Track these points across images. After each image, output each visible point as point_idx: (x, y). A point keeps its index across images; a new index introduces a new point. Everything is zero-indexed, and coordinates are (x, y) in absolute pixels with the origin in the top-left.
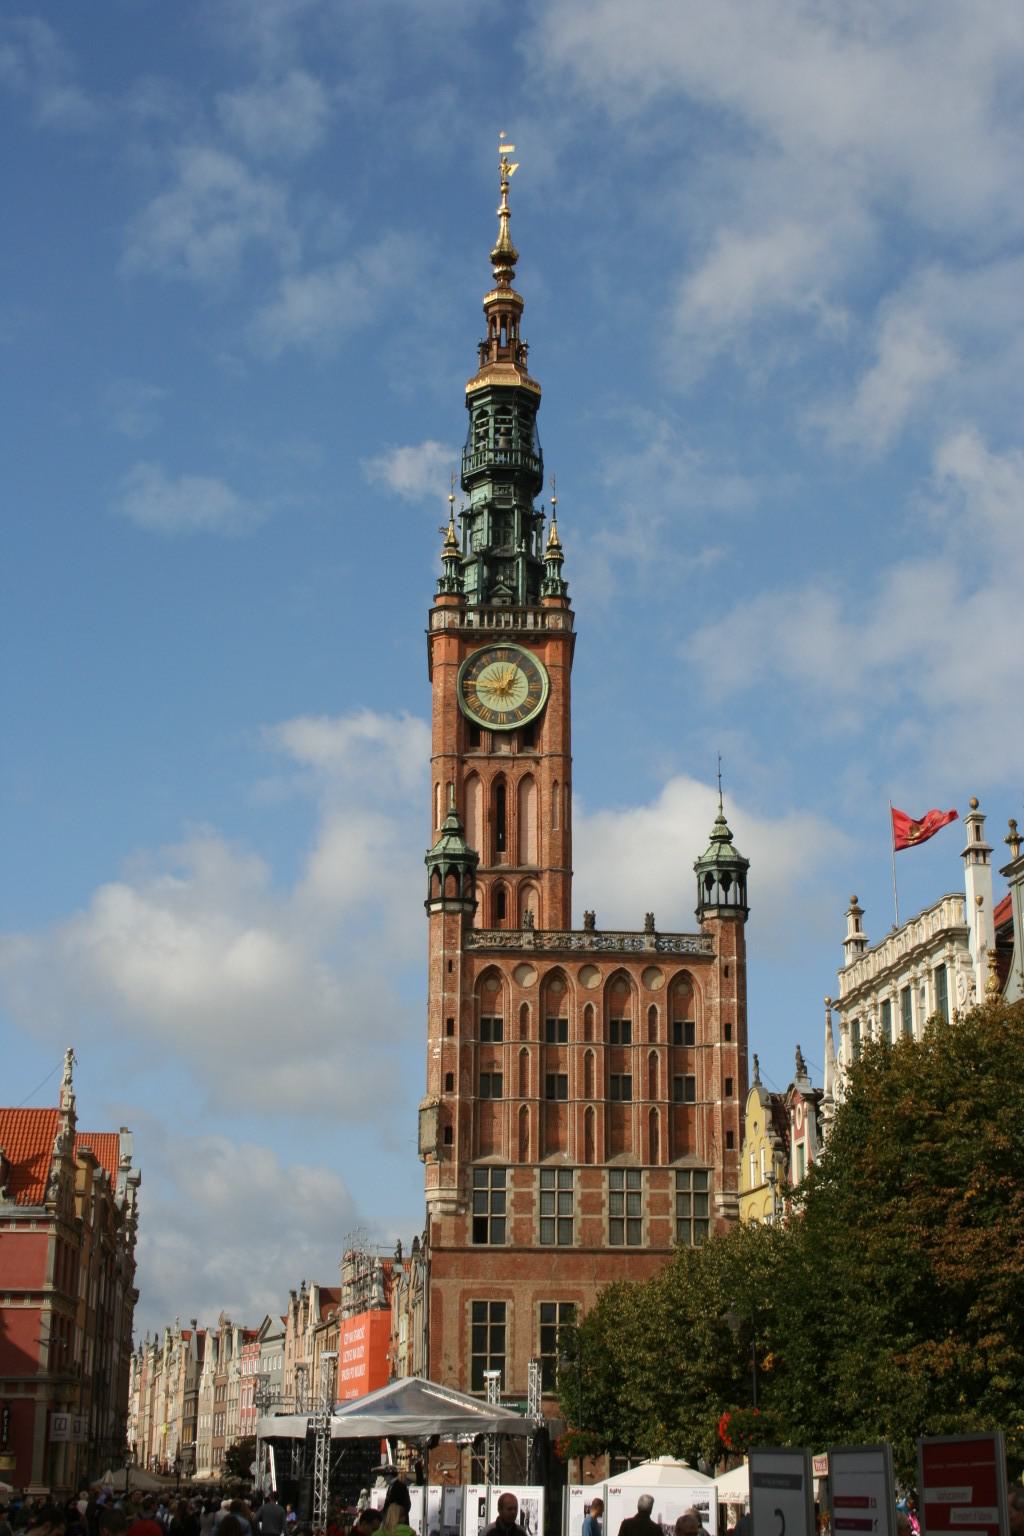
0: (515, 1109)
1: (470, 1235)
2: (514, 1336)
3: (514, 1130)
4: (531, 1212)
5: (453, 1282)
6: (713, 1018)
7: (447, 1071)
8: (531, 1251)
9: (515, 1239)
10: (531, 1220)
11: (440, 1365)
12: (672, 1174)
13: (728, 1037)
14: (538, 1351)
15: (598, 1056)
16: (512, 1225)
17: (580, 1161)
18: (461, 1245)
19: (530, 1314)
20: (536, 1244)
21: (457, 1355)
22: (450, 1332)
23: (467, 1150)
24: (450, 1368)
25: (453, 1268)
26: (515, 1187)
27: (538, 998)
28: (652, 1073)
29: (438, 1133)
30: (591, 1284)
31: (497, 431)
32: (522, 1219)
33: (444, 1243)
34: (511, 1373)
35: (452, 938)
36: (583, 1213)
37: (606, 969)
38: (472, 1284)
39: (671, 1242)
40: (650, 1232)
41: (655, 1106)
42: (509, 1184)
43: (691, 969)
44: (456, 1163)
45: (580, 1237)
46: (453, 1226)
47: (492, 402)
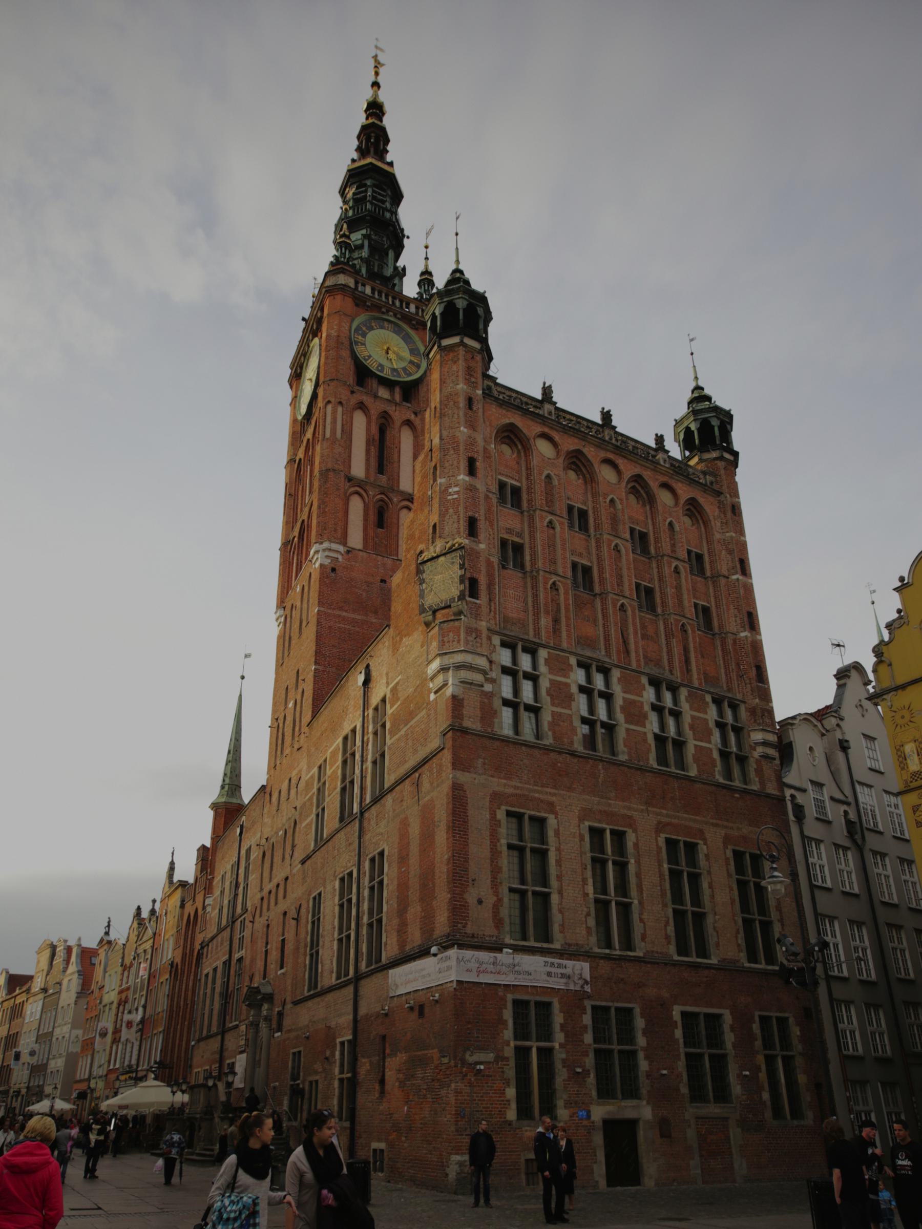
0: (546, 583)
2: (560, 866)
3: (545, 604)
7: (470, 514)
8: (573, 754)
9: (555, 738)
10: (571, 716)
11: (466, 896)
12: (708, 698)
14: (590, 889)
15: (627, 555)
16: (550, 719)
17: (619, 661)
18: (489, 730)
19: (577, 840)
20: (579, 747)
21: (489, 881)
22: (479, 850)
24: (480, 902)
28: (678, 588)
29: (462, 579)
30: (642, 811)
31: (374, 198)
32: (560, 714)
33: (467, 723)
34: (560, 916)
36: (627, 722)
37: (629, 469)
38: (505, 785)
39: (717, 777)
40: (696, 760)
41: (685, 621)
42: (543, 668)
43: (701, 500)
44: (484, 624)
45: (625, 750)
47: (371, 178)
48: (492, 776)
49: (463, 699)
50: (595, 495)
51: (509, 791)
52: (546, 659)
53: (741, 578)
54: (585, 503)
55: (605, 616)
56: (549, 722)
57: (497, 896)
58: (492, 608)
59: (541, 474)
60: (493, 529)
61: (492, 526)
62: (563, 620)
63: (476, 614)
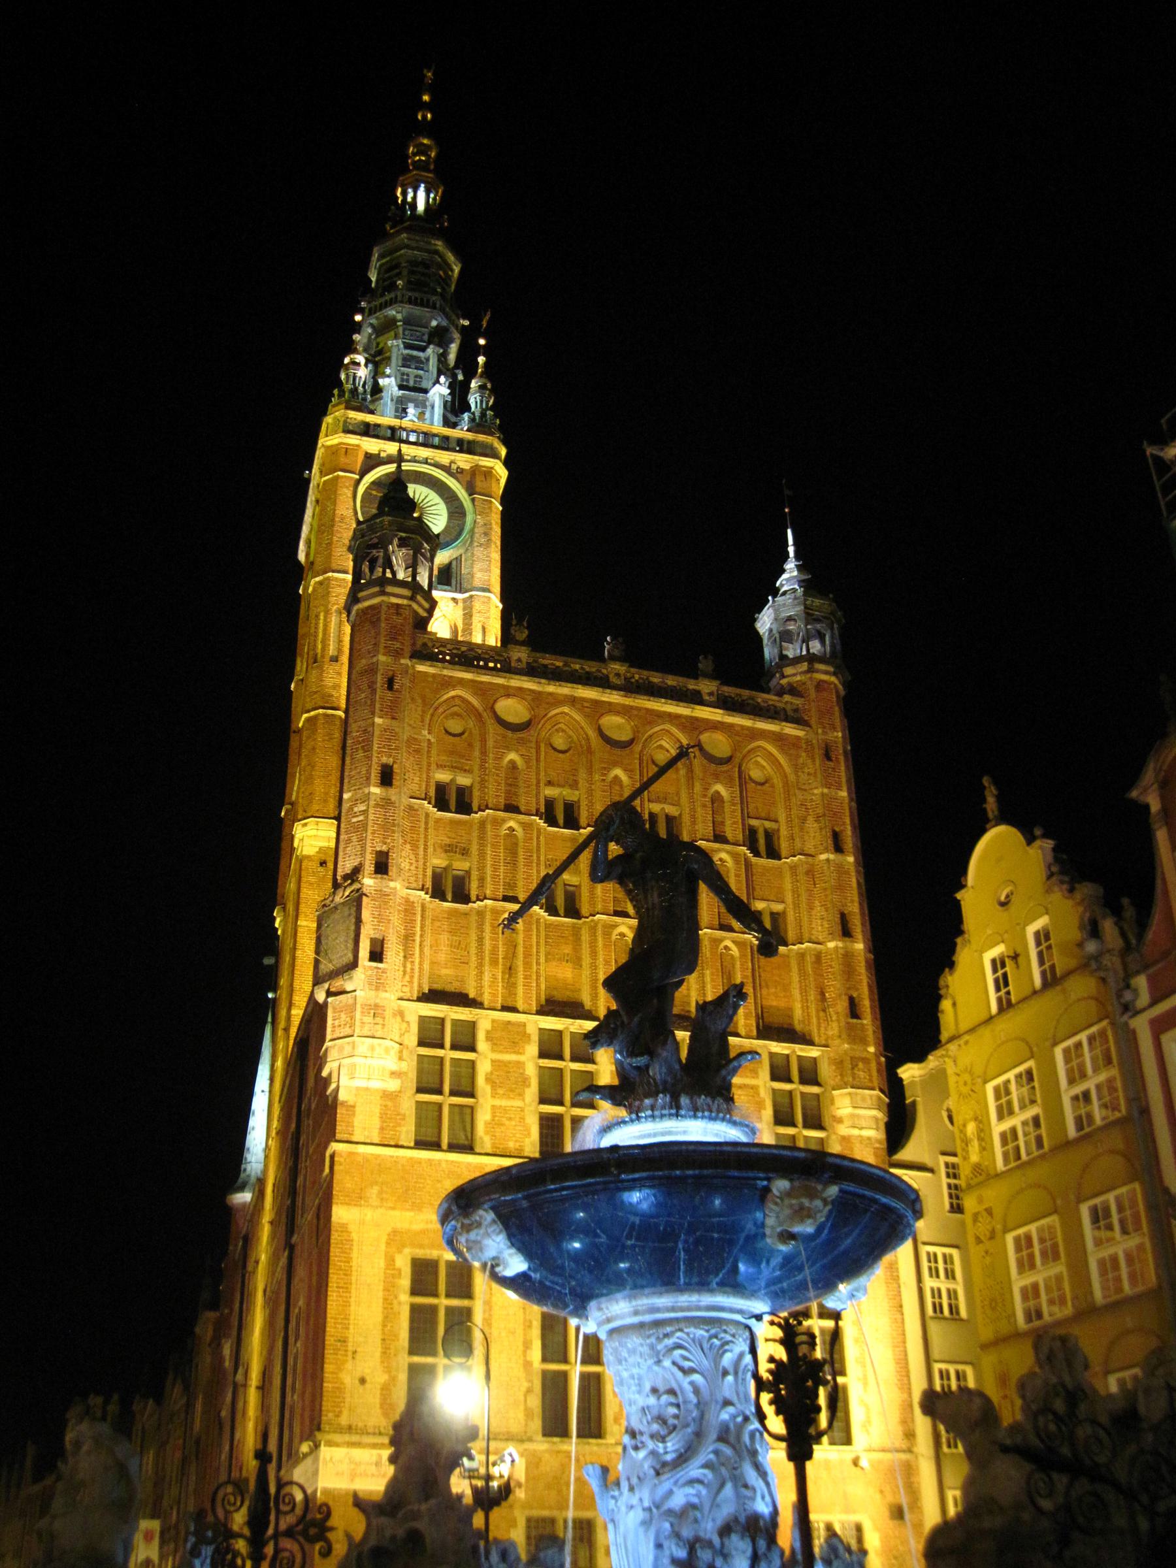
1: (407, 1132)
3: (494, 950)
4: (521, 1095)
5: (369, 1214)
6: (810, 819)
13: (838, 848)
14: (536, 1354)
16: (488, 1117)
21: (378, 1354)
23: (407, 978)
25: (375, 1190)
26: (493, 1050)
27: (533, 751)
32: (505, 1110)
35: (394, 639)
46: (377, 1110)
48: (393, 1208)
49: (354, 1107)
50: (590, 771)
51: (416, 1227)
52: (488, 1032)
53: (832, 856)
54: (574, 785)
55: (594, 954)
56: (487, 1124)
57: (389, 1372)
58: (408, 970)
59: (499, 758)
60: (416, 855)
61: (415, 848)
62: (521, 968)
63: (378, 985)
